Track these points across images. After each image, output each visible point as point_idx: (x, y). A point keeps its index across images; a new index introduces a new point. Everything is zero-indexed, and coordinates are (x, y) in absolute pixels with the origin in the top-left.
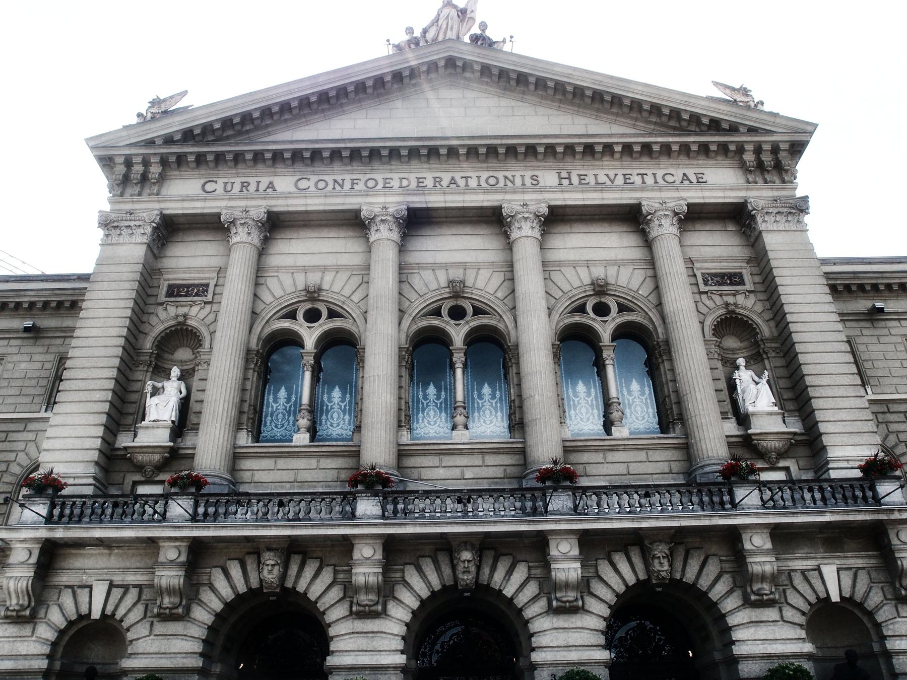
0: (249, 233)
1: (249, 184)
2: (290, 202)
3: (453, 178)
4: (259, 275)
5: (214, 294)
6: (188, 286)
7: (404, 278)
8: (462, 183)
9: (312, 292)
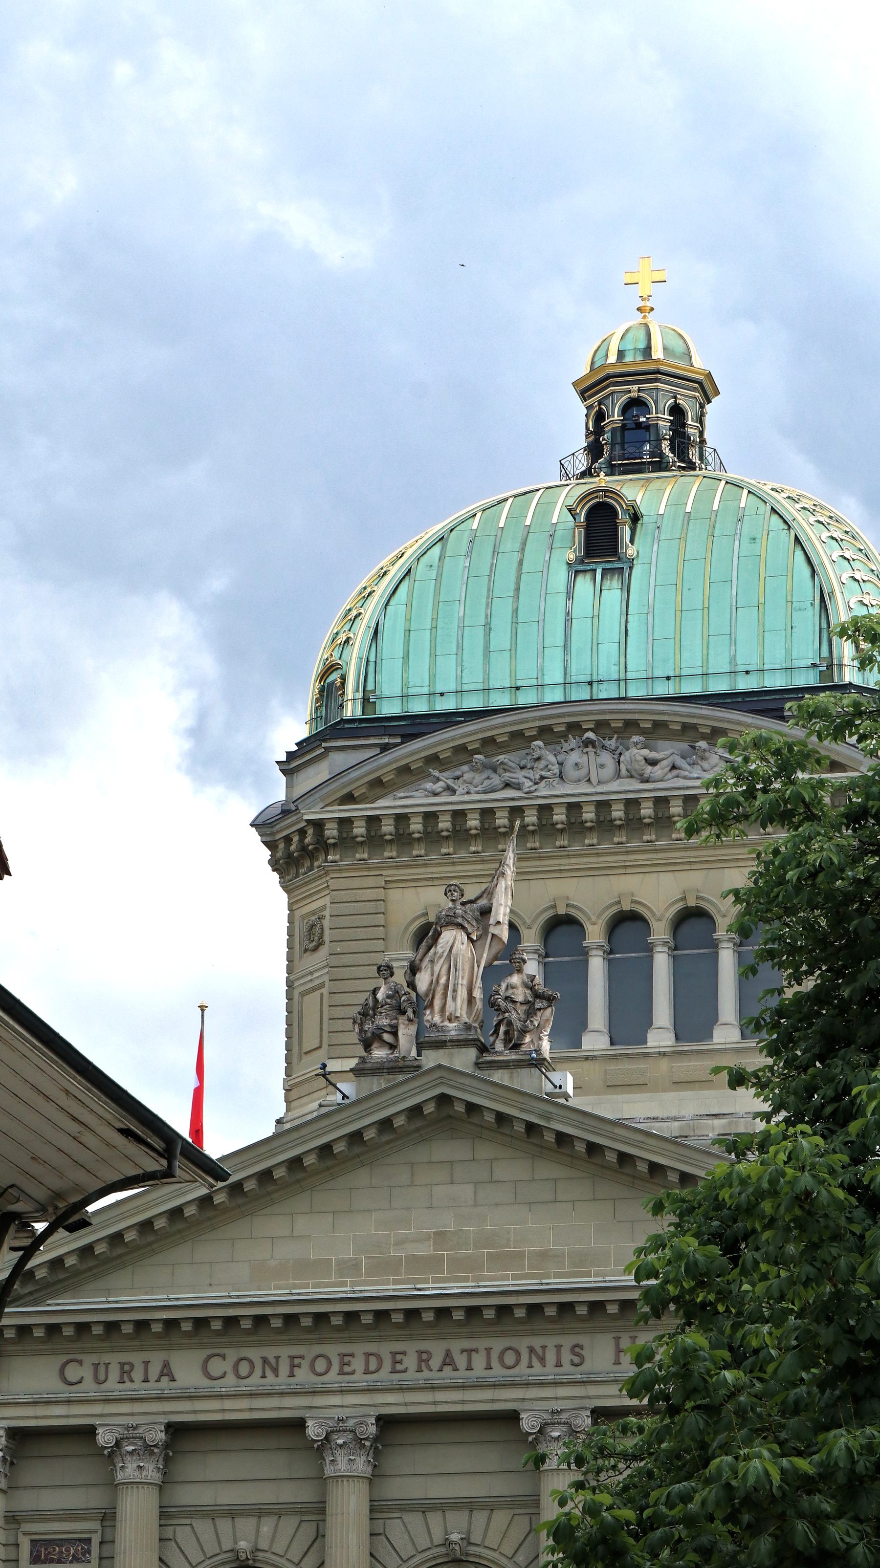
0: (140, 1467)
1: (132, 1366)
2: (200, 1405)
3: (448, 1353)
4: (163, 1522)
5: (101, 1558)
6: (60, 1542)
7: (379, 1527)
8: (461, 1361)
9: (243, 1561)
